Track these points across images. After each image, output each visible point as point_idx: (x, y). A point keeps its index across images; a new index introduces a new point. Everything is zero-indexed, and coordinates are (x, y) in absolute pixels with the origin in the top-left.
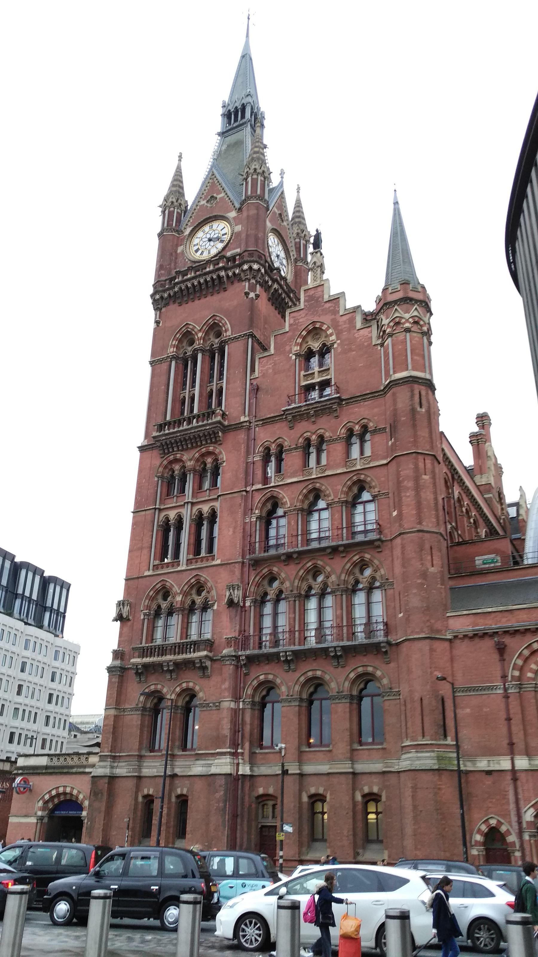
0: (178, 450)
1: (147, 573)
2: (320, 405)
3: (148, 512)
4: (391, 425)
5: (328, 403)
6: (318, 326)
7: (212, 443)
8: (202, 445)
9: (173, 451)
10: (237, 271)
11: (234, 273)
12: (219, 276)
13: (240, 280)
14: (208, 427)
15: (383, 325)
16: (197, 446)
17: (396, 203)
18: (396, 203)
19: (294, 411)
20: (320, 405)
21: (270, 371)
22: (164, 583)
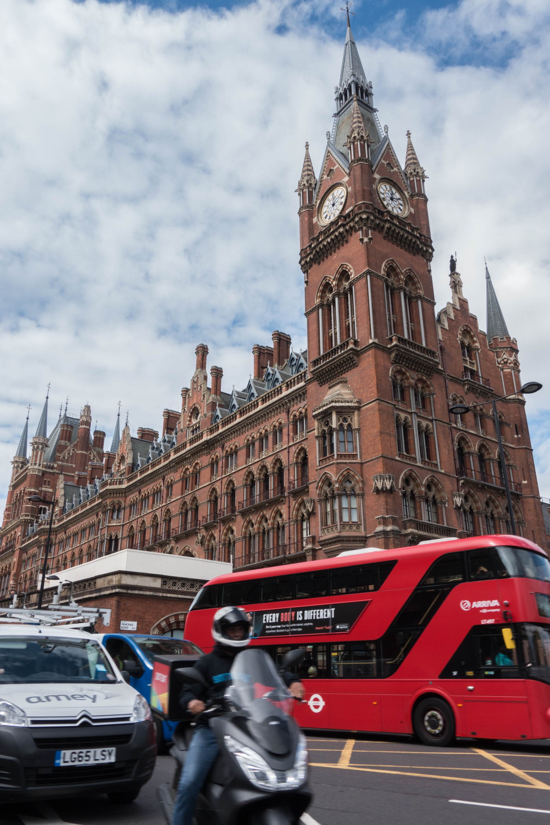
0: (405, 365)
1: (397, 458)
2: (484, 389)
3: (389, 405)
4: (516, 425)
5: (488, 391)
6: (469, 329)
7: (426, 374)
8: (420, 372)
9: (401, 364)
10: (425, 249)
11: (422, 248)
12: (416, 242)
13: (423, 256)
14: (431, 363)
15: (505, 358)
16: (417, 371)
17: (488, 277)
18: (488, 277)
19: (472, 384)
20: (484, 389)
21: (448, 342)
22: (411, 472)
